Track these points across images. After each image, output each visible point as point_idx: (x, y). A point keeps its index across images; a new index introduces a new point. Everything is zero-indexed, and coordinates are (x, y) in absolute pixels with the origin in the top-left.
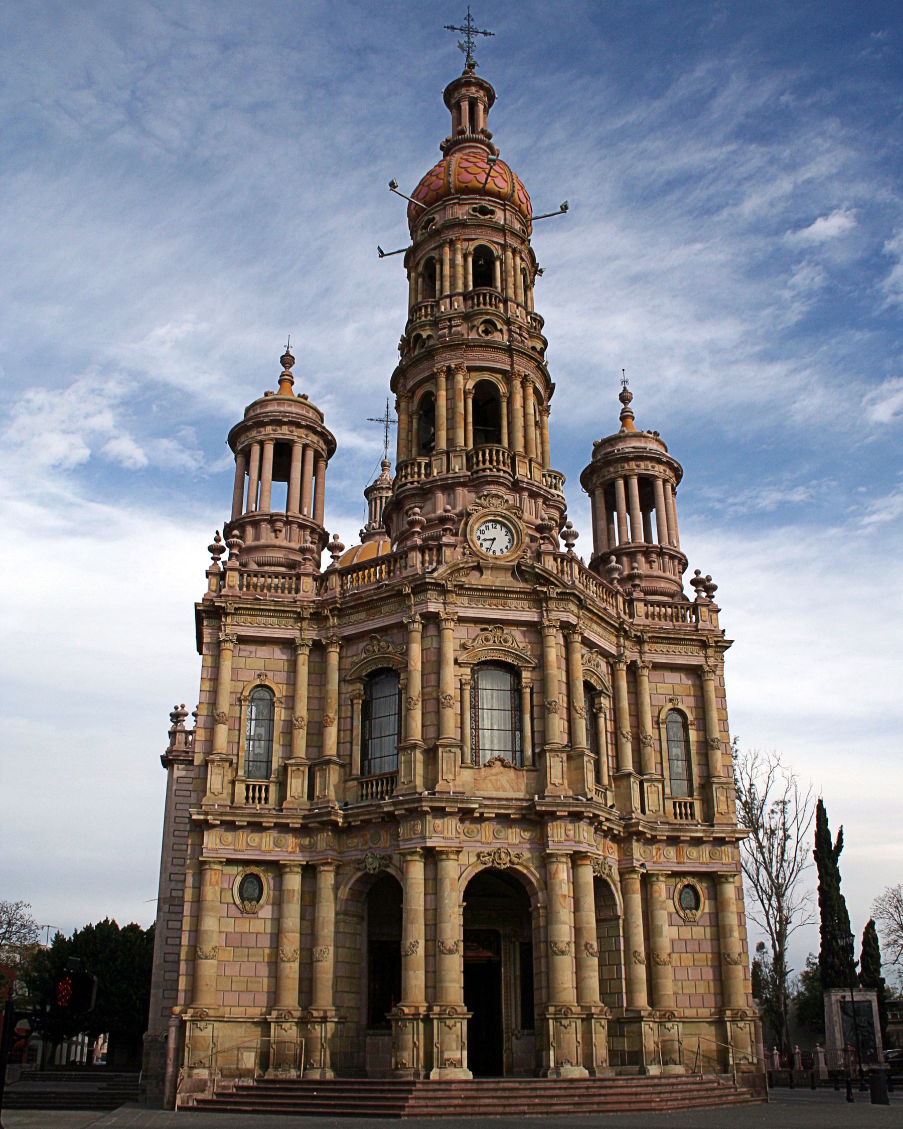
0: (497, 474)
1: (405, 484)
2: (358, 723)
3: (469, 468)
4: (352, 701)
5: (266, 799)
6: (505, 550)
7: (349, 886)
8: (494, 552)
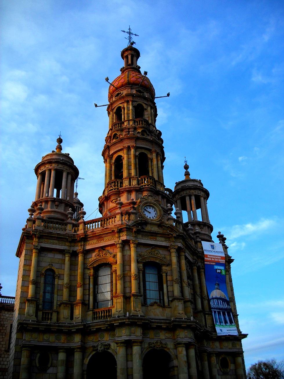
0: (150, 187)
1: (112, 190)
2: (91, 286)
3: (138, 185)
4: (89, 277)
6: (154, 218)
7: (89, 358)
8: (150, 218)
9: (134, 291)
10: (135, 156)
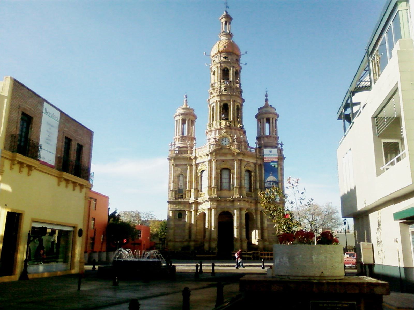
3: (220, 125)
5: (183, 197)
9: (213, 185)
10: (220, 107)
